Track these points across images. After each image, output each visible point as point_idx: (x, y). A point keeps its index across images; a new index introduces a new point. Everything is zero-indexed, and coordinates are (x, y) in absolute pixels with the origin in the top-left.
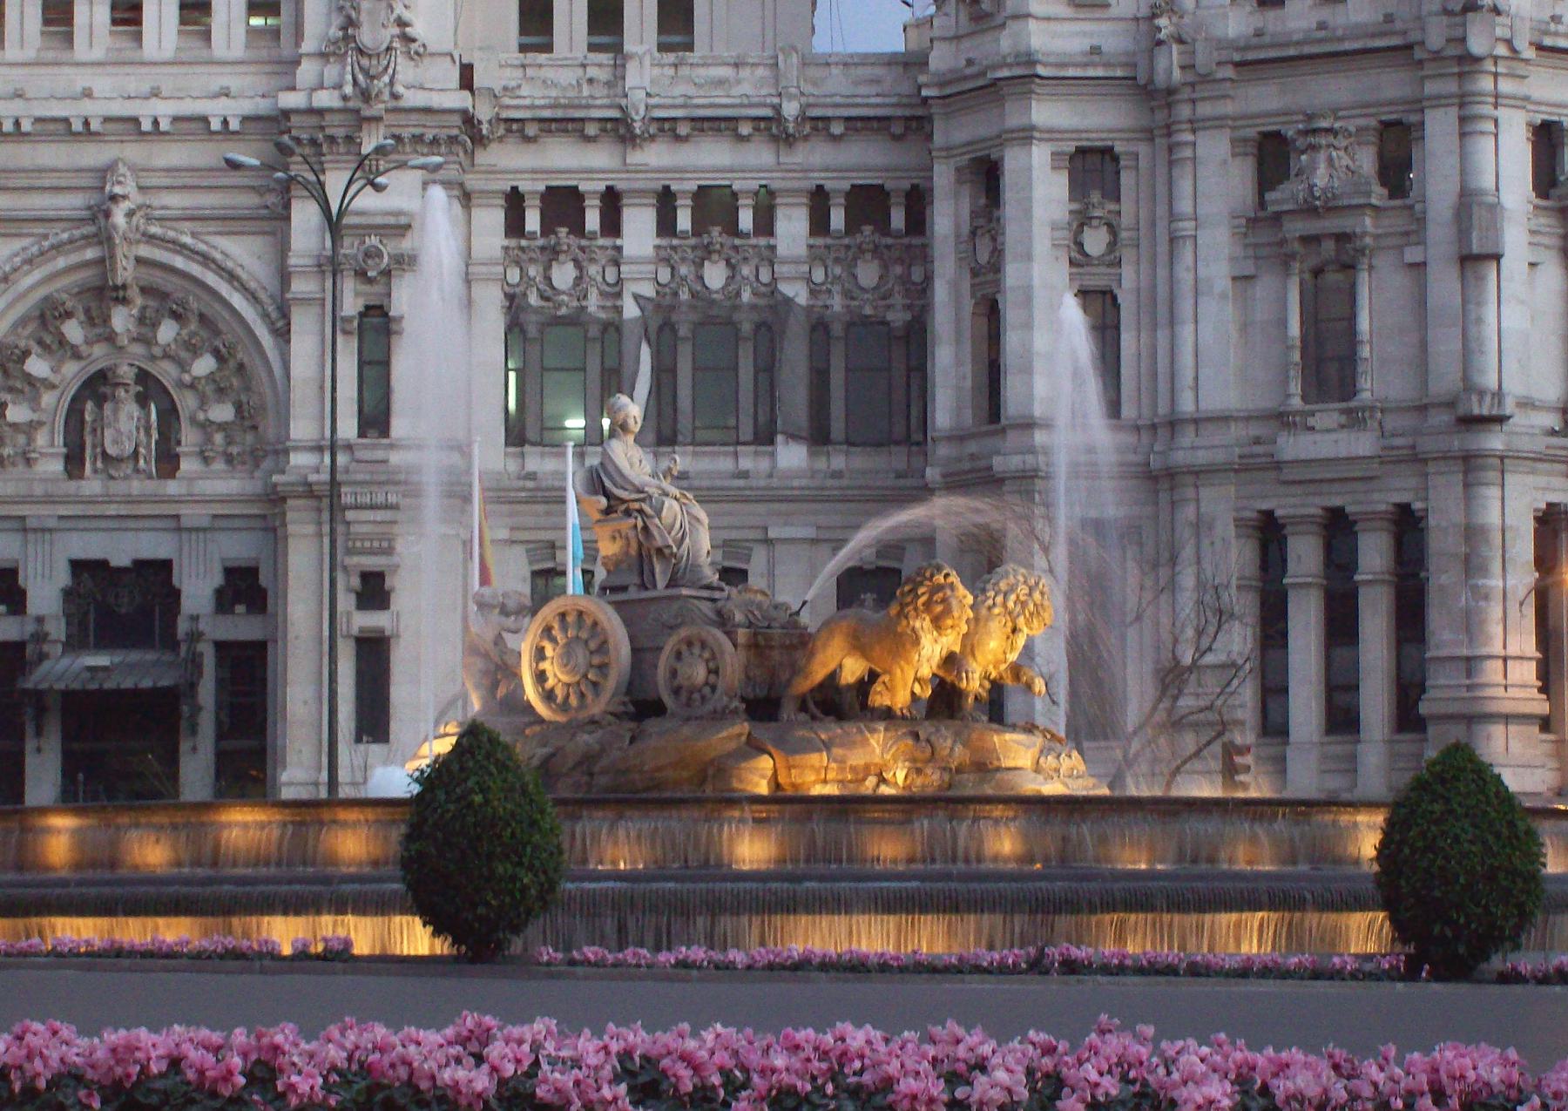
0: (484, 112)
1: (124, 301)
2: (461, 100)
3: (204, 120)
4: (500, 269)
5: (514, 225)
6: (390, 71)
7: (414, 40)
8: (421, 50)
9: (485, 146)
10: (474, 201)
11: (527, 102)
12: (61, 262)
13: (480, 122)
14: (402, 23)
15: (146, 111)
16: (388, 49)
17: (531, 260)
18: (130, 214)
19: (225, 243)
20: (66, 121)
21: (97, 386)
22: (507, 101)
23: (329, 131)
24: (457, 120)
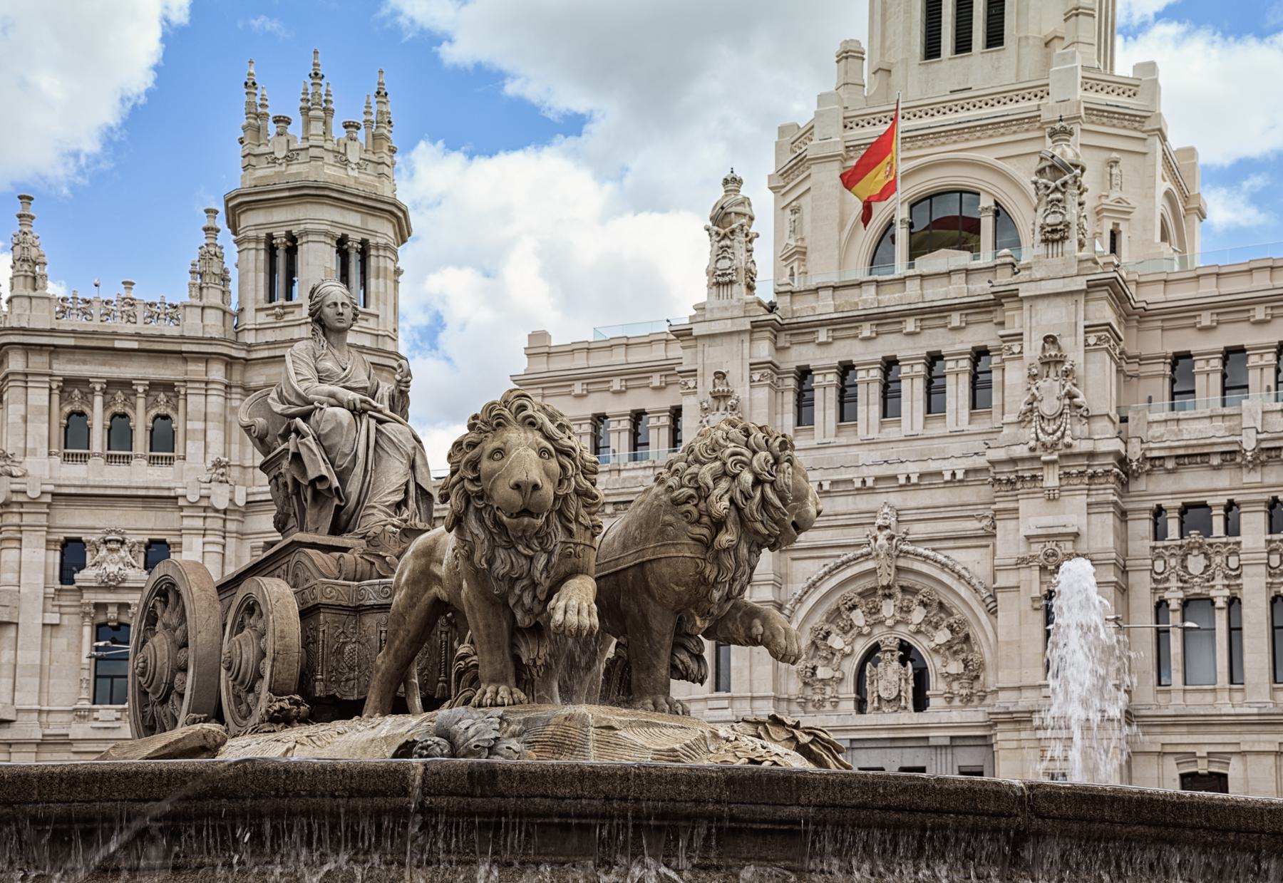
0: (1135, 452)
1: (890, 596)
2: (1117, 445)
3: (940, 474)
4: (1149, 562)
5: (1159, 533)
6: (1062, 429)
7: (1080, 407)
8: (1085, 414)
9: (1137, 478)
10: (1129, 517)
11: (1167, 444)
12: (849, 573)
13: (1131, 460)
14: (1071, 396)
15: (901, 471)
16: (1061, 414)
17: (1173, 555)
18: (891, 538)
19: (954, 555)
20: (851, 481)
21: (872, 654)
22: (1152, 445)
23: (1020, 474)
24: (1111, 460)
